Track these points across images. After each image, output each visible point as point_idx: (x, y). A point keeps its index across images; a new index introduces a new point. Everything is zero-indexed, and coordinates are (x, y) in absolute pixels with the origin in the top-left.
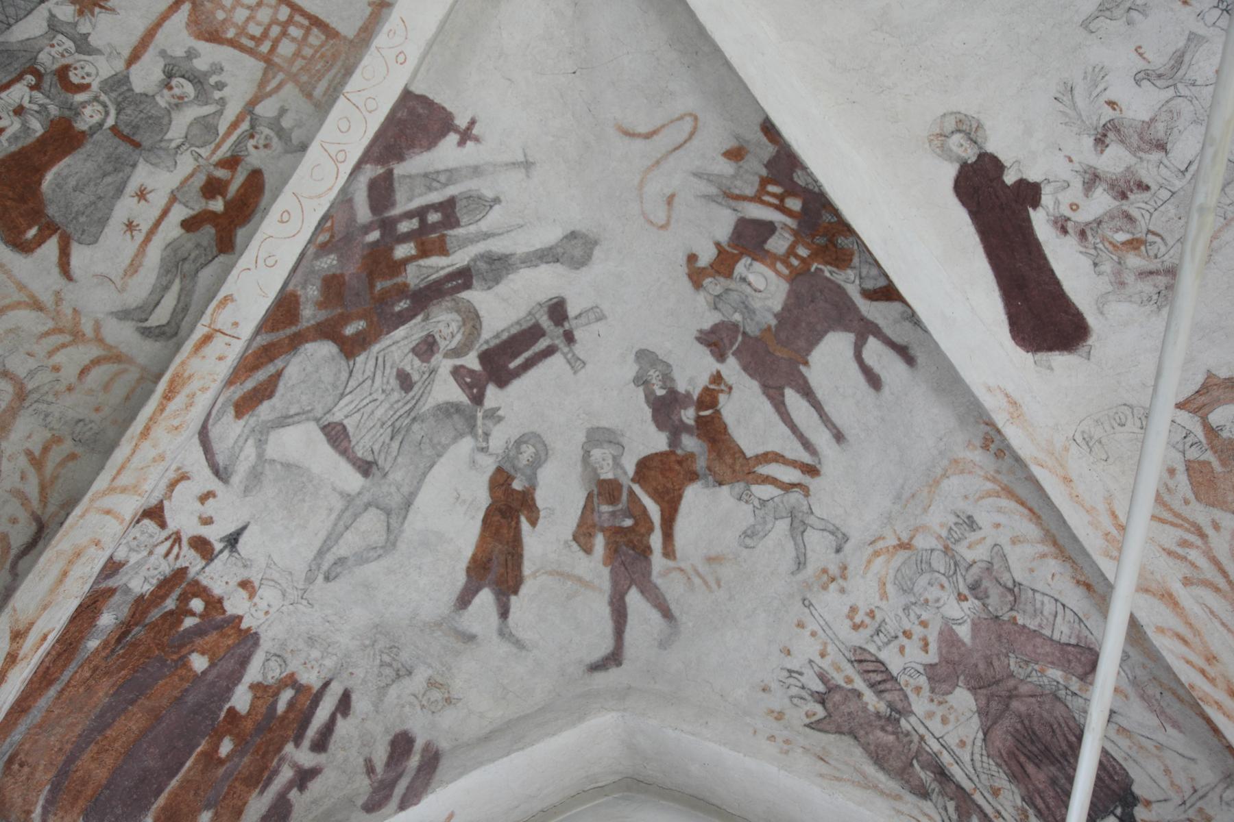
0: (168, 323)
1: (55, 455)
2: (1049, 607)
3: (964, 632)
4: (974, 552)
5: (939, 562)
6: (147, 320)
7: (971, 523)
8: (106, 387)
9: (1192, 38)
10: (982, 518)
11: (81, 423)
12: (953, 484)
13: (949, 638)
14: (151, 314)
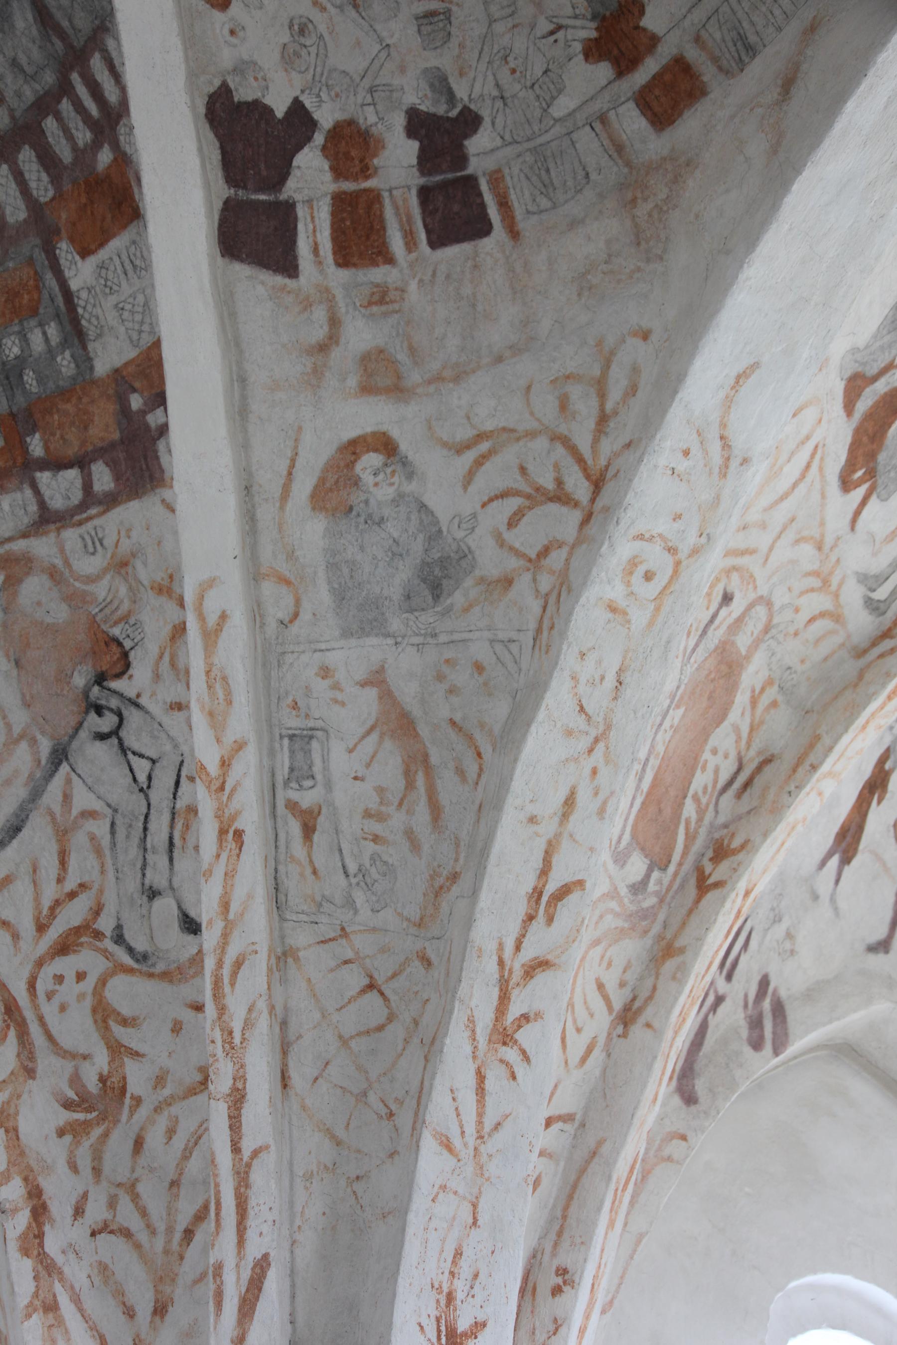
0: (885, 600)
1: (764, 701)
6: (874, 590)
8: (817, 641)
11: (788, 672)
14: (880, 585)
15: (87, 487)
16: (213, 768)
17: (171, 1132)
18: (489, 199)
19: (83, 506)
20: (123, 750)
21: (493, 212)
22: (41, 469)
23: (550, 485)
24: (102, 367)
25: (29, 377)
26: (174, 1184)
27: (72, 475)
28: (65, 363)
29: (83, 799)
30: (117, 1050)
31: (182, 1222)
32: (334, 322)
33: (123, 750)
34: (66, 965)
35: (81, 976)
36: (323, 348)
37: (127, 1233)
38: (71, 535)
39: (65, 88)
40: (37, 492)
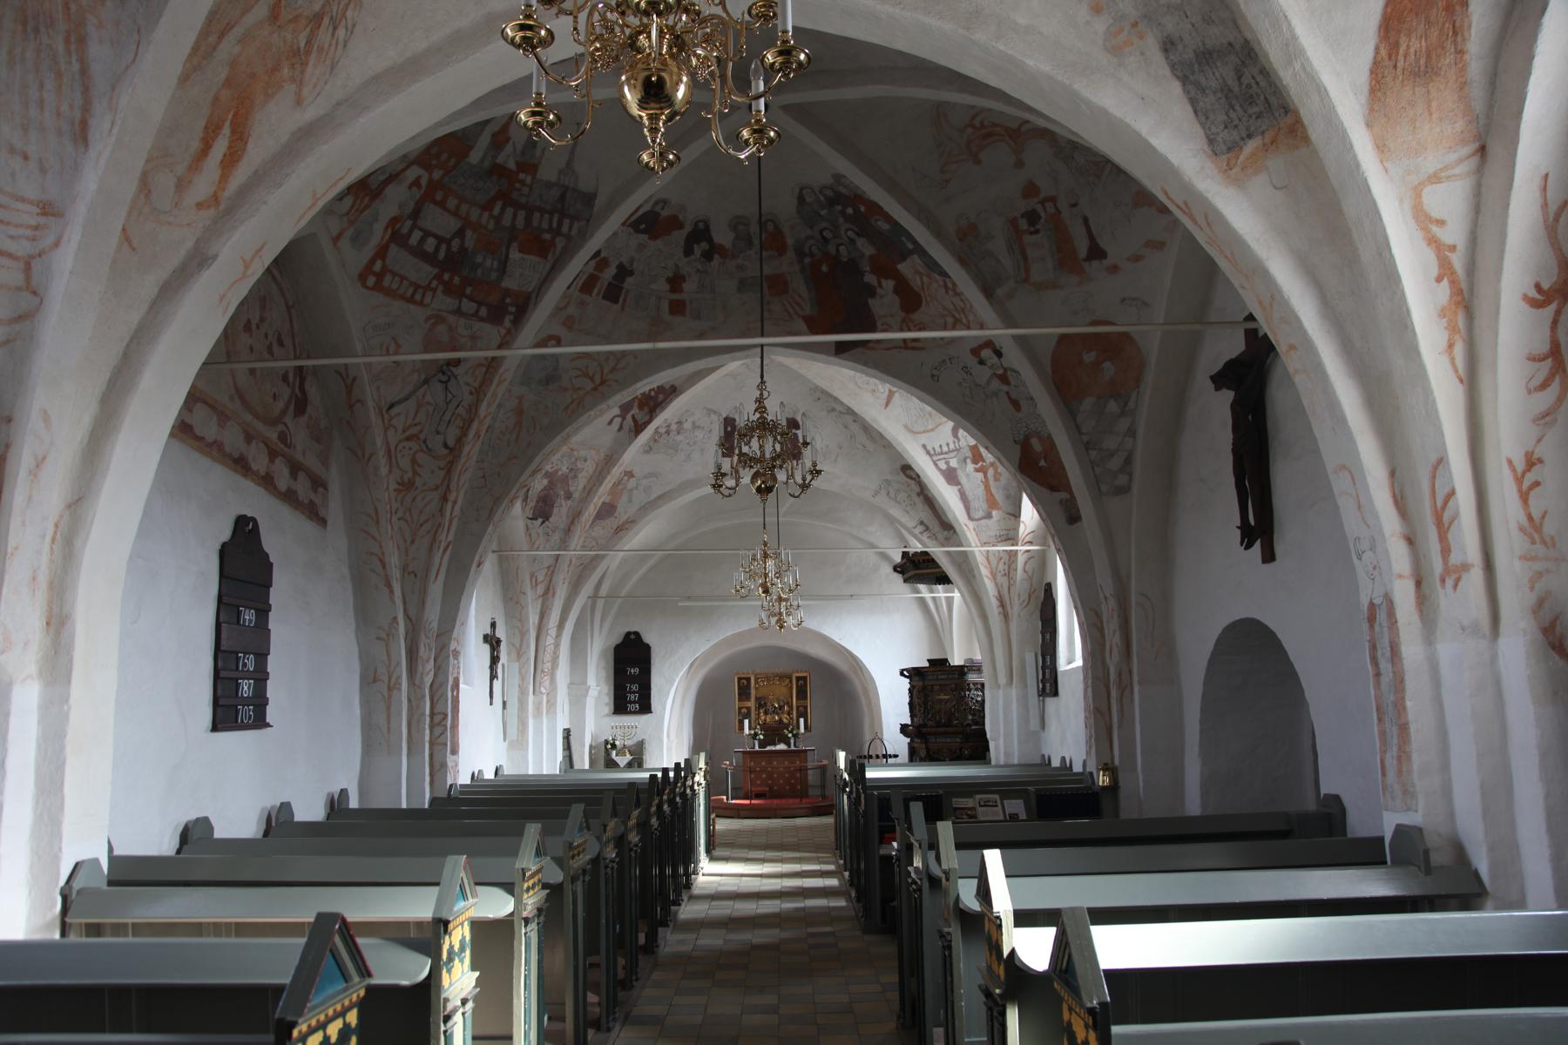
2: (576, 484)
3: (560, 473)
4: (579, 465)
5: (573, 459)
7: (586, 460)
9: (703, 428)
10: (588, 462)
12: (593, 452)
13: (557, 471)
15: (477, 311)
16: (482, 417)
17: (423, 499)
18: (622, 297)
19: (473, 315)
20: (446, 388)
21: (621, 300)
22: (466, 298)
23: (591, 374)
24: (504, 284)
25: (479, 272)
26: (421, 512)
27: (475, 305)
28: (494, 276)
29: (428, 398)
30: (415, 473)
31: (421, 522)
32: (568, 303)
33: (446, 388)
34: (407, 444)
35: (410, 449)
36: (561, 309)
37: (407, 521)
38: (462, 321)
39: (551, 213)
40: (460, 303)
